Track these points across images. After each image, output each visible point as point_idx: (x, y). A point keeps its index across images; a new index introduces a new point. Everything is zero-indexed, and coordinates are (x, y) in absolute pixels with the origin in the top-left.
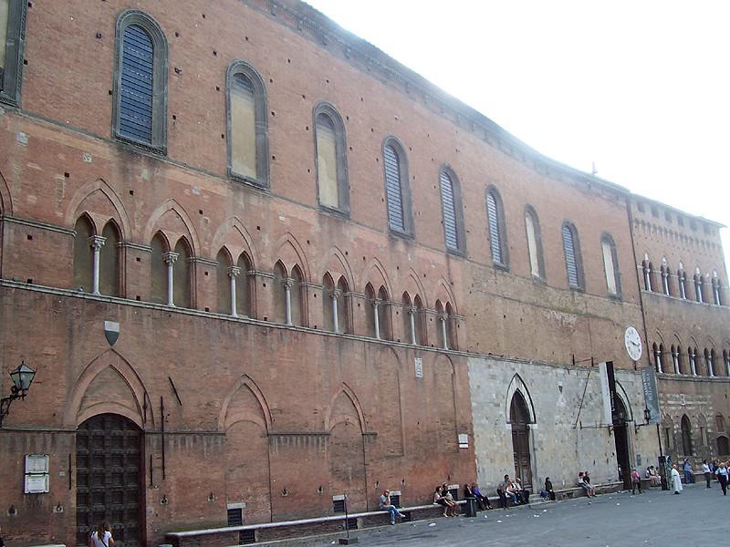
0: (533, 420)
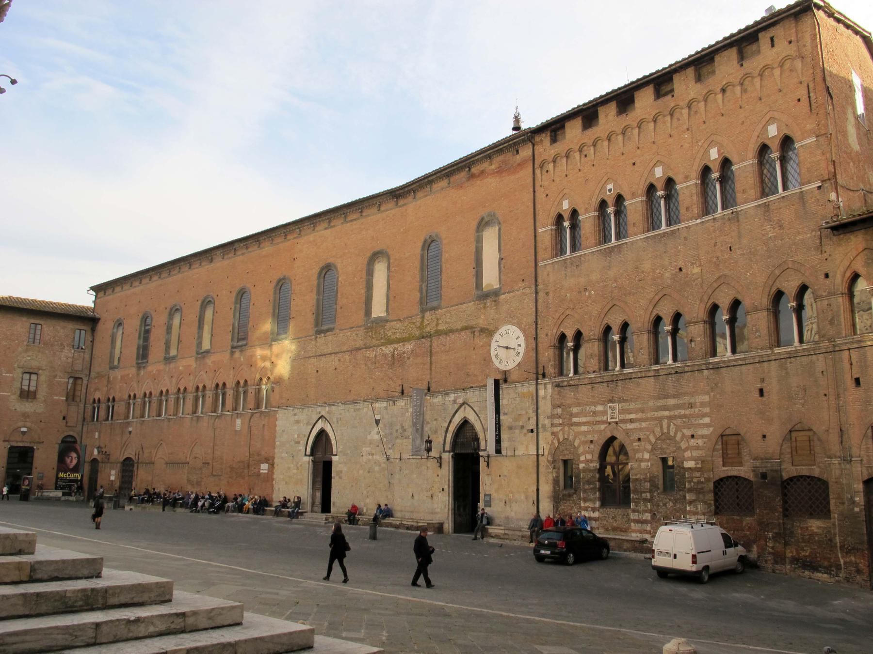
0: (335, 453)
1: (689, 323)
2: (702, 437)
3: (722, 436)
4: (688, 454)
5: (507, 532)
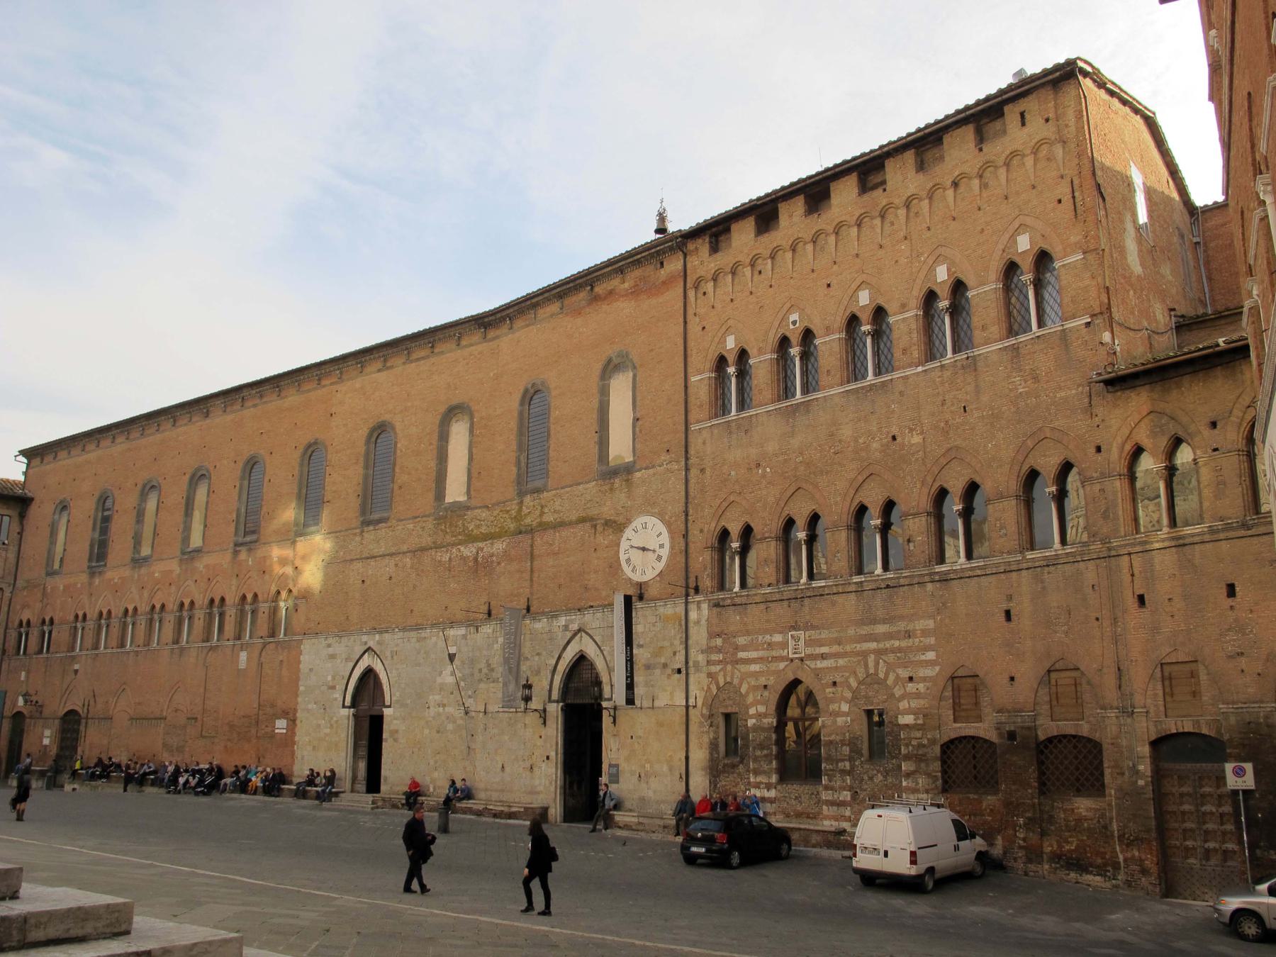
0: (387, 703)
1: (905, 515)
2: (924, 679)
3: (953, 678)
4: (904, 705)
5: (641, 820)
